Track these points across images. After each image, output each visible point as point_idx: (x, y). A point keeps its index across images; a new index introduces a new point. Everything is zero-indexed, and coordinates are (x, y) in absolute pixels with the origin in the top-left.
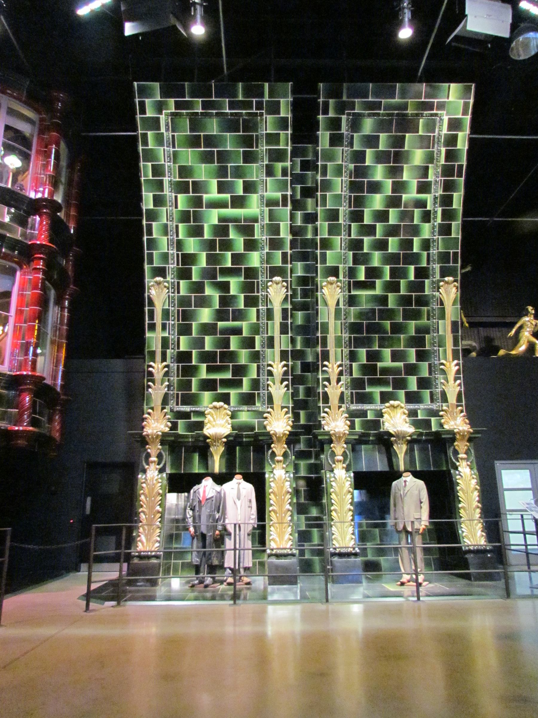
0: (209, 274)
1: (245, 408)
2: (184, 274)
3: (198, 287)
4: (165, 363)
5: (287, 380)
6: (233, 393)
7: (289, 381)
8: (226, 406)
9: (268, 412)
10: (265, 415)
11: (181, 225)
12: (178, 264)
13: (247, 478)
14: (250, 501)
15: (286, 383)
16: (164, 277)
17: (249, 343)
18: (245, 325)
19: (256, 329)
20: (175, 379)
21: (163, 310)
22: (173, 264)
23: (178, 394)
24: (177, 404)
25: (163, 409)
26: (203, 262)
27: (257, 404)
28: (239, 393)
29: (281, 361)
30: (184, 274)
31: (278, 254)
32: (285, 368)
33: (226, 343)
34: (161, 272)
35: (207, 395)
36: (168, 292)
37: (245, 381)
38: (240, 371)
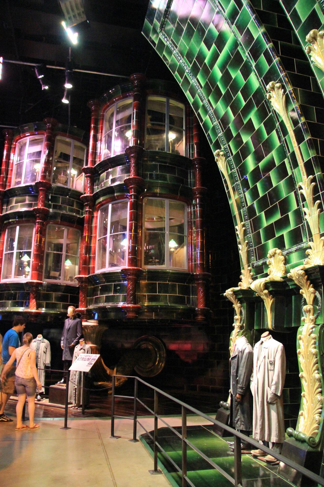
0: (239, 122)
1: (295, 248)
2: (228, 136)
3: (239, 141)
4: (242, 223)
5: (318, 198)
6: (285, 233)
7: (320, 200)
8: (278, 251)
9: (310, 248)
10: (308, 251)
11: (210, 98)
12: (223, 131)
13: (276, 335)
14: (273, 363)
15: (318, 201)
16: (220, 148)
17: (282, 172)
18: (274, 154)
19: (283, 152)
20: (251, 235)
21: (229, 175)
22: (220, 132)
23: (255, 249)
24: (257, 260)
25: (249, 266)
26: (232, 117)
27: (304, 240)
28: (289, 232)
29: (308, 176)
30: (228, 136)
31: (262, 57)
32: (313, 184)
33: (268, 183)
34: (217, 146)
35: (270, 243)
36: (226, 159)
37: (291, 215)
38: (284, 206)
